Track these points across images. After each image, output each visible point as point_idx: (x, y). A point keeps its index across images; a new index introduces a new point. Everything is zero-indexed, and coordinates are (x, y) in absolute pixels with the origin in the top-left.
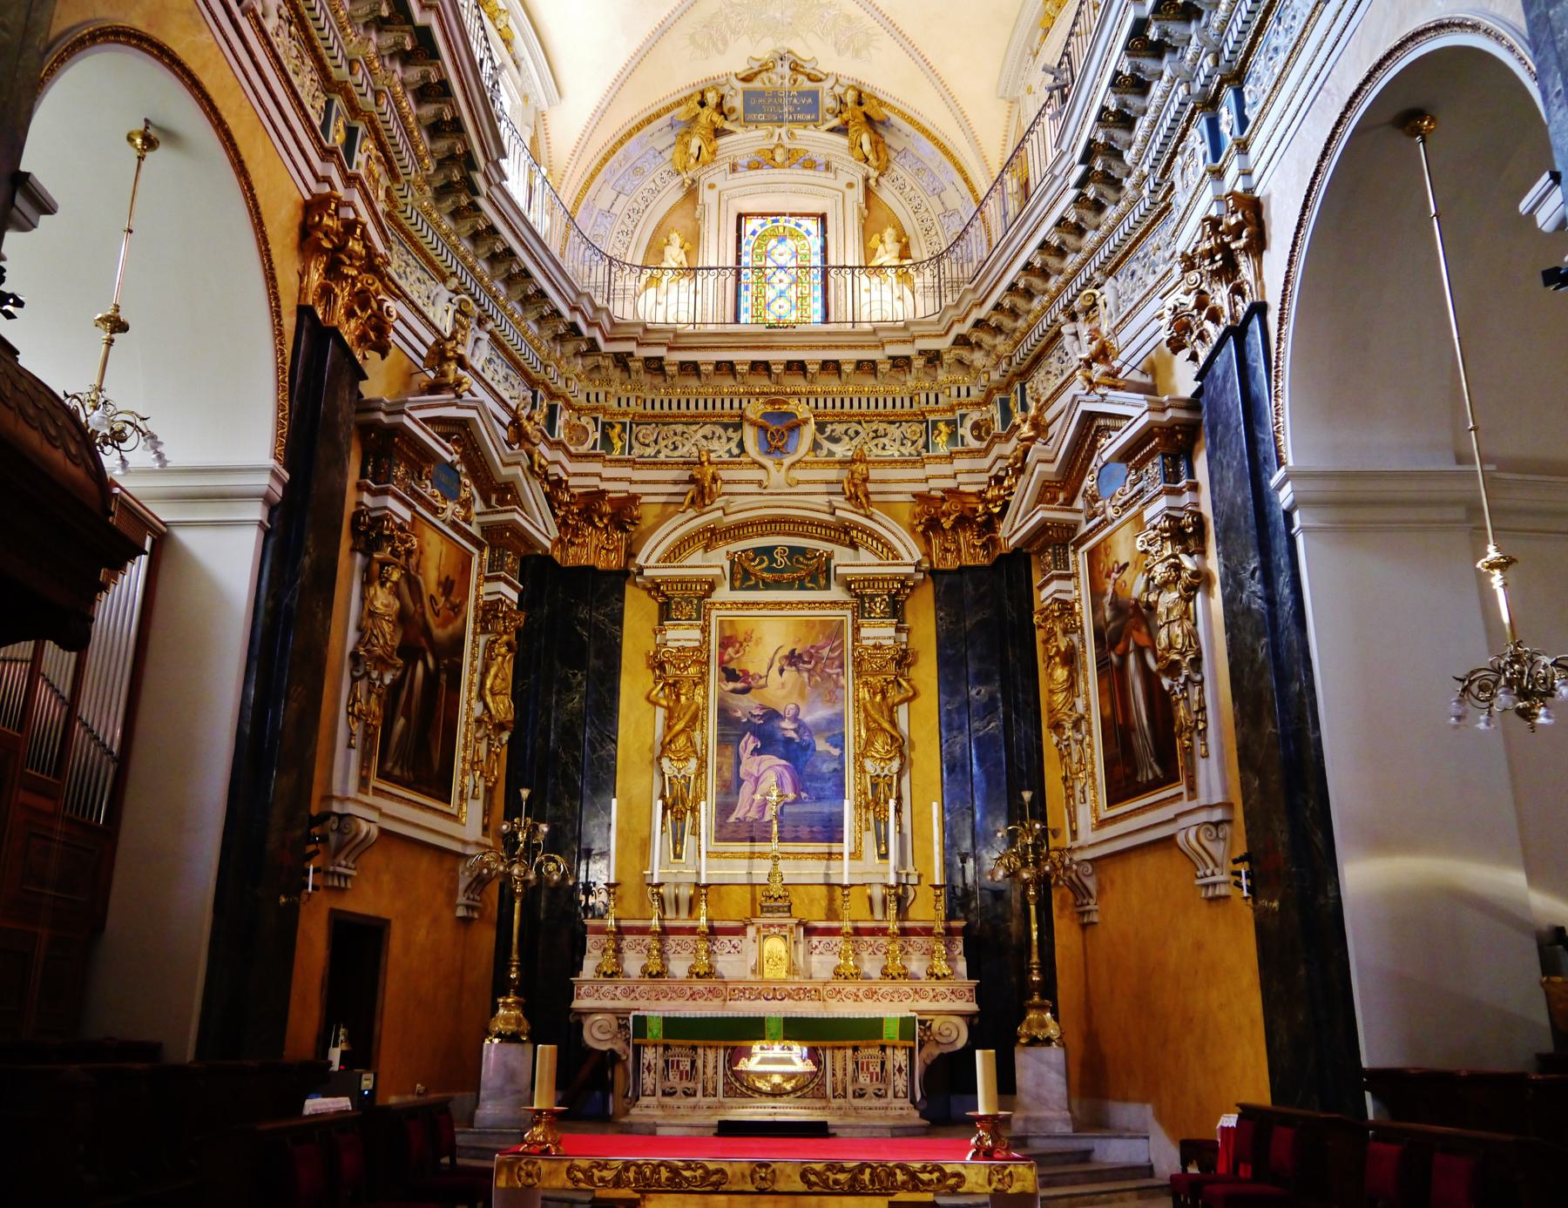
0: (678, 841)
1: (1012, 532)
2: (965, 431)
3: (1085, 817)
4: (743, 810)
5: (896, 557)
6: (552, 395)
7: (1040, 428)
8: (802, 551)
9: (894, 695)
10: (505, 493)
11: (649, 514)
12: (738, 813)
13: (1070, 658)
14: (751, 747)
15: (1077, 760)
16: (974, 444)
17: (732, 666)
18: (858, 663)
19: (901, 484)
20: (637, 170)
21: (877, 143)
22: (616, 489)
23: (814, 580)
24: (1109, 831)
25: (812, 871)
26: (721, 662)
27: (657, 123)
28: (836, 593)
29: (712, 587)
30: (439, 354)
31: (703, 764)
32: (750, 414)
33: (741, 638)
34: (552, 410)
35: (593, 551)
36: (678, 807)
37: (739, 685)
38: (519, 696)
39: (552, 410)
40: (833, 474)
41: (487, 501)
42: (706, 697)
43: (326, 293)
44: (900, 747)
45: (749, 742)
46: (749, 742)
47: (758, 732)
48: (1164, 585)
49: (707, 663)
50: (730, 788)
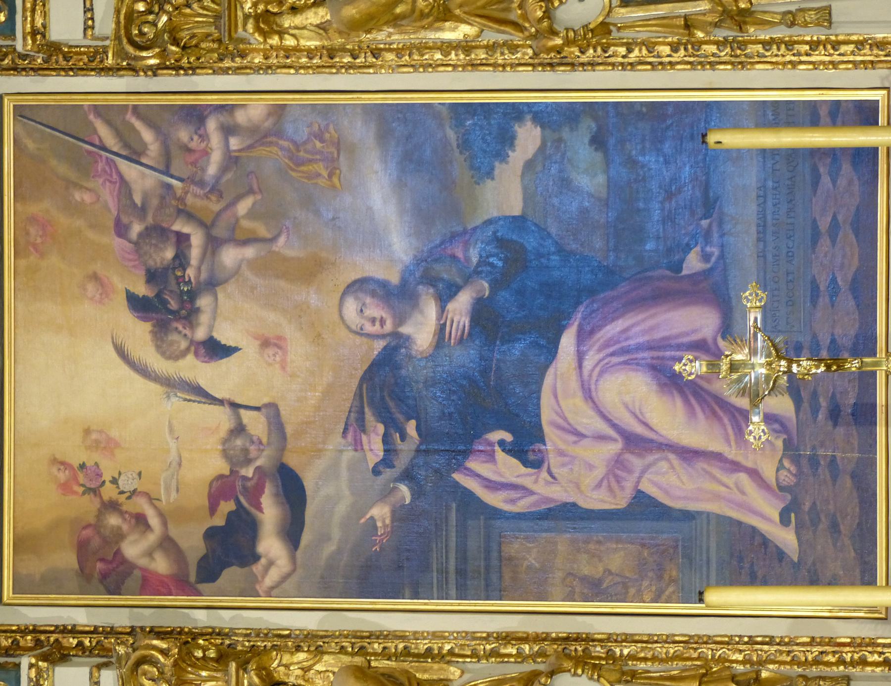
12: (764, 514)
14: (508, 467)
17: (193, 542)
18: (183, 53)
26: (180, 584)
33: (87, 506)
37: (270, 513)
42: (314, 643)
45: (492, 473)
47: (455, 441)
49: (185, 638)
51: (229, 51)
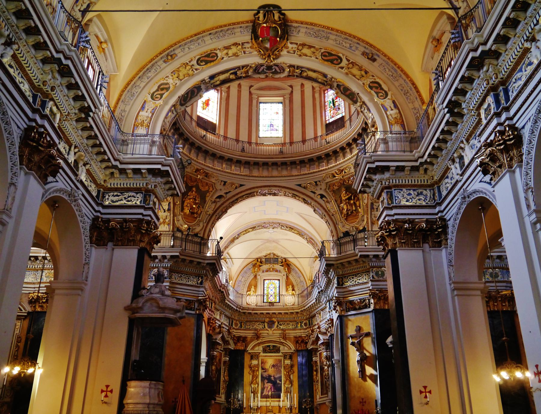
0: (254, 398)
1: (310, 347)
2: (303, 325)
3: (318, 397)
4: (265, 393)
6: (232, 319)
7: (313, 331)
9: (290, 373)
11: (249, 339)
13: (317, 371)
15: (318, 387)
16: (305, 327)
18: (284, 367)
19: (293, 334)
20: (246, 272)
21: (288, 269)
24: (321, 400)
25: (276, 404)
28: (280, 354)
30: (220, 326)
31: (258, 385)
35: (240, 347)
36: (254, 392)
38: (230, 375)
39: (232, 321)
40: (280, 332)
43: (210, 330)
44: (291, 382)
45: (266, 381)
46: (266, 381)
47: (267, 379)
48: (326, 365)
50: (263, 389)
51: (284, 369)
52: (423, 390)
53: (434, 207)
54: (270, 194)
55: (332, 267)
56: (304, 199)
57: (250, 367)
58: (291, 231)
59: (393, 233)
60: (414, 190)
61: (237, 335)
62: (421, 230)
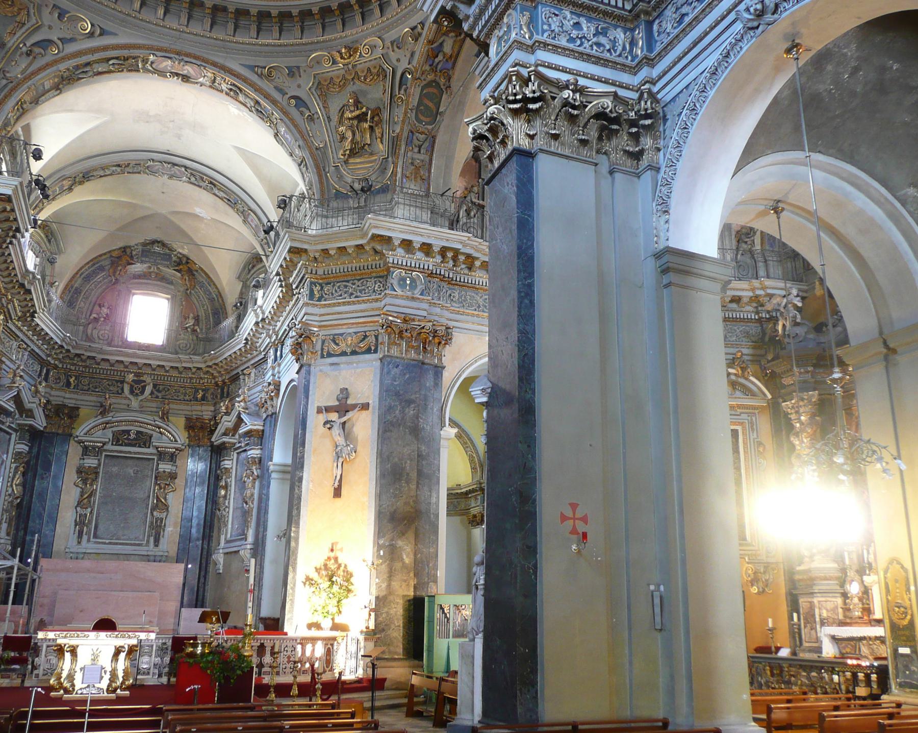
1: (217, 438)
5: (176, 441)
8: (141, 433)
10: (30, 414)
22: (70, 403)
23: (145, 444)
27: (104, 257)
28: (151, 450)
29: (104, 444)
32: (127, 380)
34: (48, 371)
39: (48, 371)
41: (22, 416)
52: (569, 513)
53: (634, 70)
54: (177, 75)
55: (304, 257)
56: (257, 102)
57: (80, 471)
58: (210, 191)
59: (531, 106)
60: (589, 19)
61: (55, 401)
62: (601, 115)
